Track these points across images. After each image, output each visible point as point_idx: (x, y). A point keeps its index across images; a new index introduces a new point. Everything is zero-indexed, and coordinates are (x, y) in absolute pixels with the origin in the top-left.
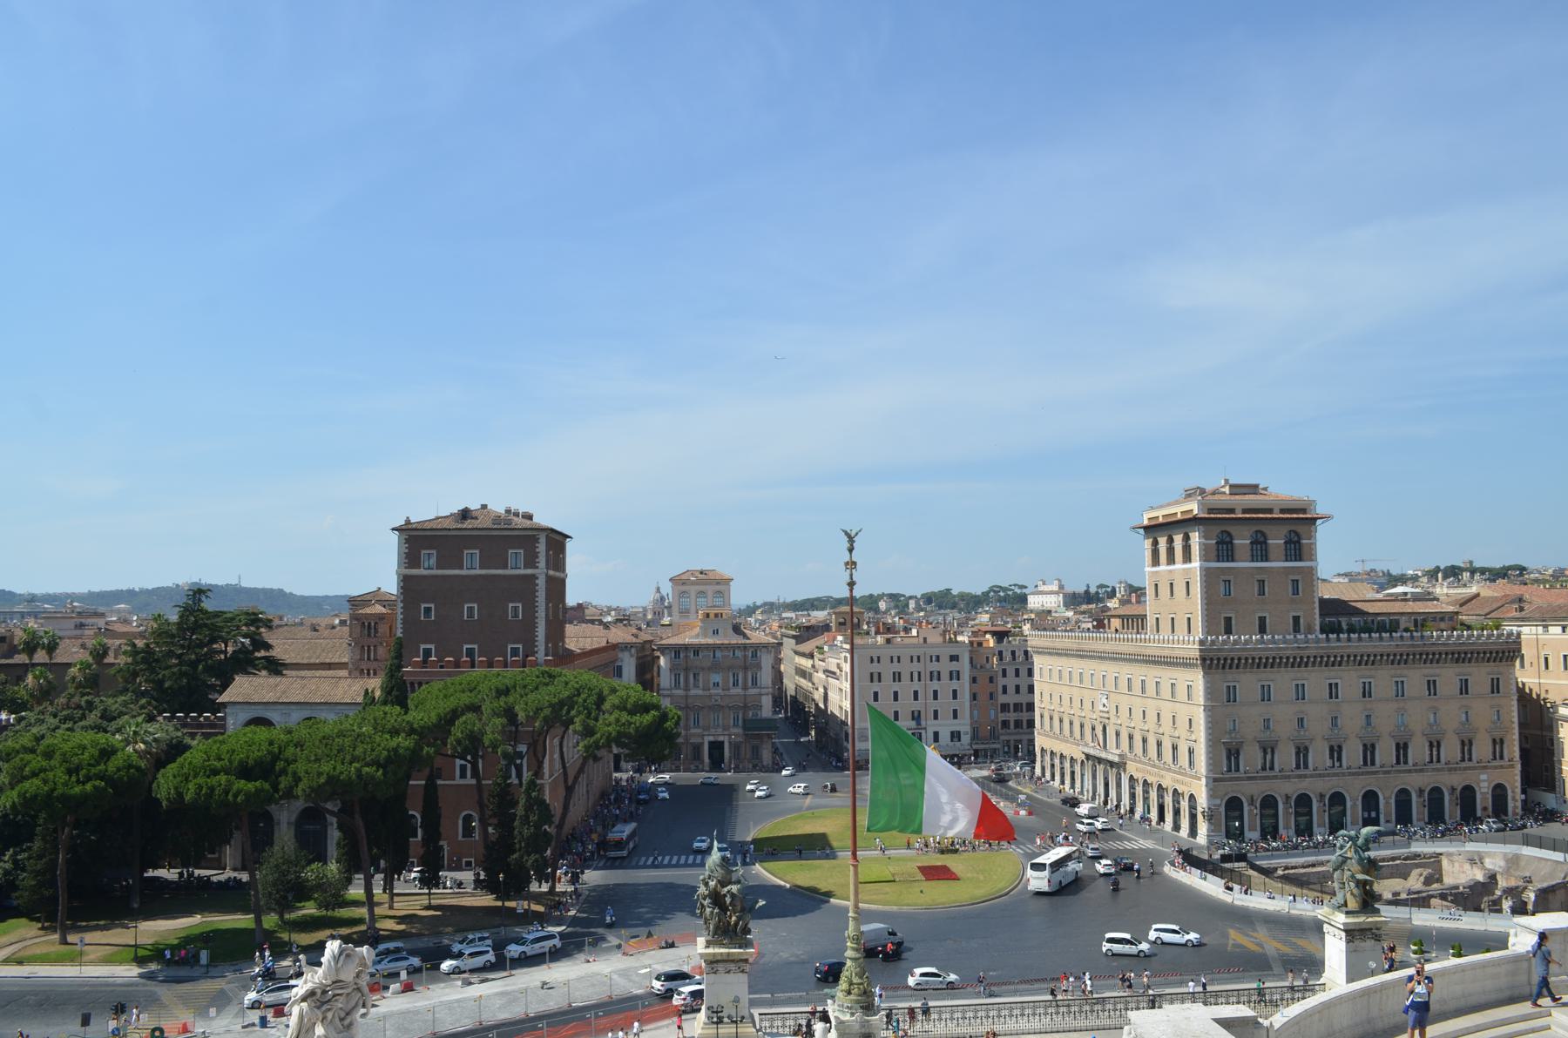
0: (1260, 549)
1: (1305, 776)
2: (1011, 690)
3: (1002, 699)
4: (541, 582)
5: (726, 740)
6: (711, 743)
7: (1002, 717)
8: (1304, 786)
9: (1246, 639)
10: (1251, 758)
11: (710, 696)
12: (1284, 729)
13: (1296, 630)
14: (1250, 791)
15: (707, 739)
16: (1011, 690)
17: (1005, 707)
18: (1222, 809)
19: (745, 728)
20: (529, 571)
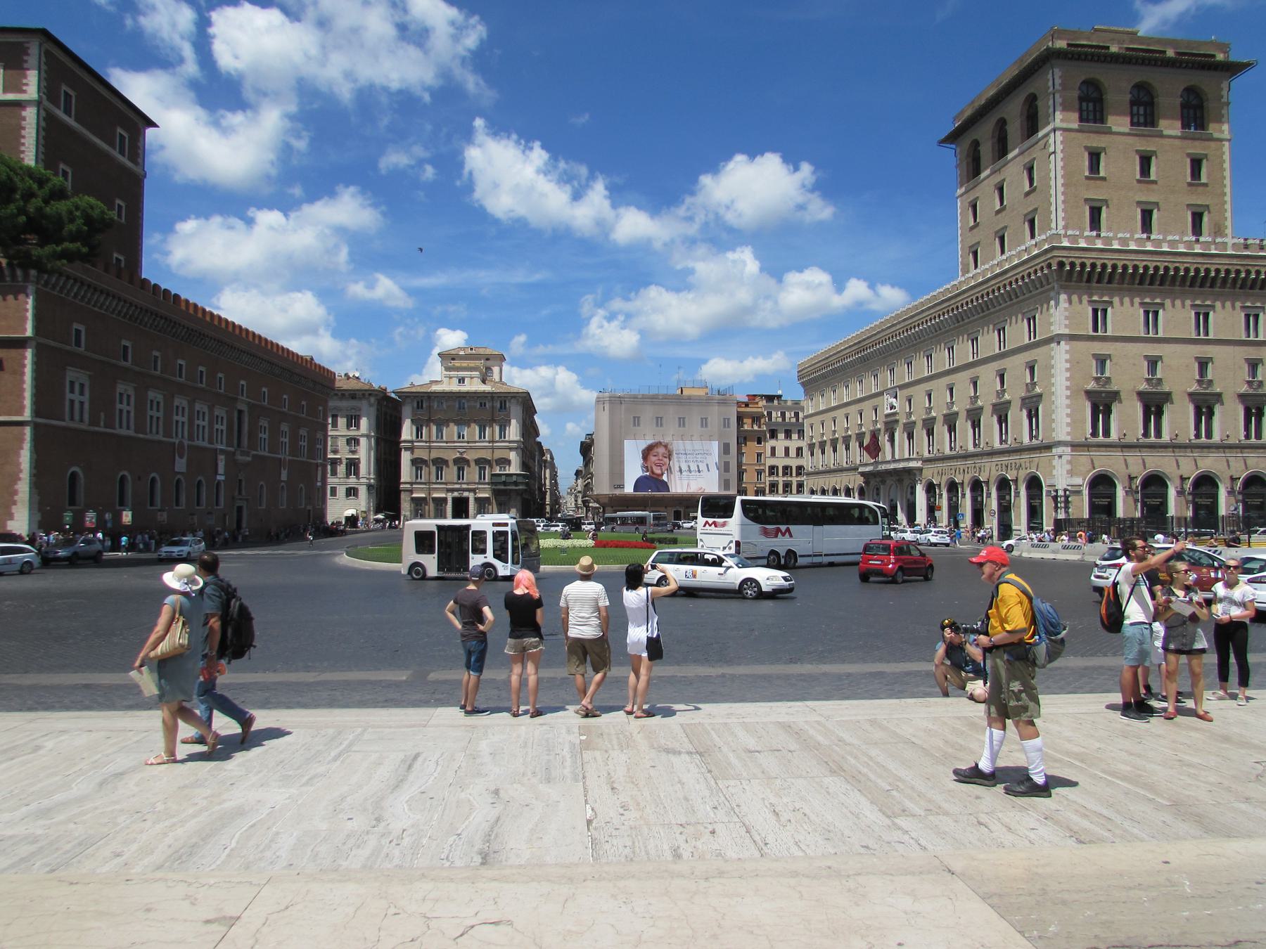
0: (1145, 112)
1: (1208, 447)
2: (780, 452)
3: (770, 462)
4: (30, 114)
5: (471, 496)
6: (454, 499)
7: (767, 479)
8: (1209, 463)
9: (1121, 238)
10: (1127, 419)
11: (455, 448)
12: (1179, 376)
13: (1197, 230)
14: (1127, 468)
15: (450, 496)
16: (780, 452)
17: (773, 470)
18: (1086, 492)
19: (491, 483)
20: (11, 97)
